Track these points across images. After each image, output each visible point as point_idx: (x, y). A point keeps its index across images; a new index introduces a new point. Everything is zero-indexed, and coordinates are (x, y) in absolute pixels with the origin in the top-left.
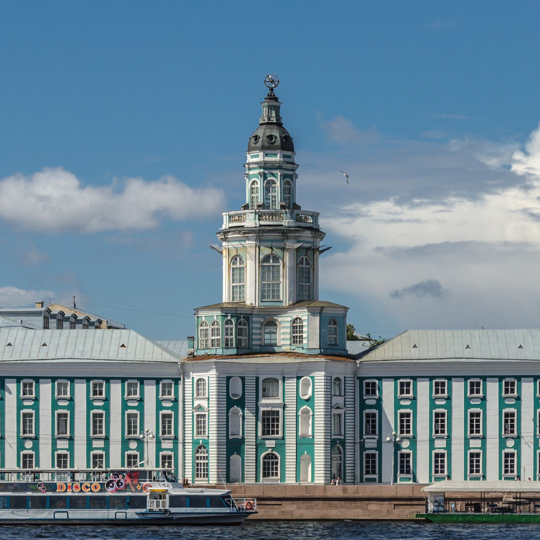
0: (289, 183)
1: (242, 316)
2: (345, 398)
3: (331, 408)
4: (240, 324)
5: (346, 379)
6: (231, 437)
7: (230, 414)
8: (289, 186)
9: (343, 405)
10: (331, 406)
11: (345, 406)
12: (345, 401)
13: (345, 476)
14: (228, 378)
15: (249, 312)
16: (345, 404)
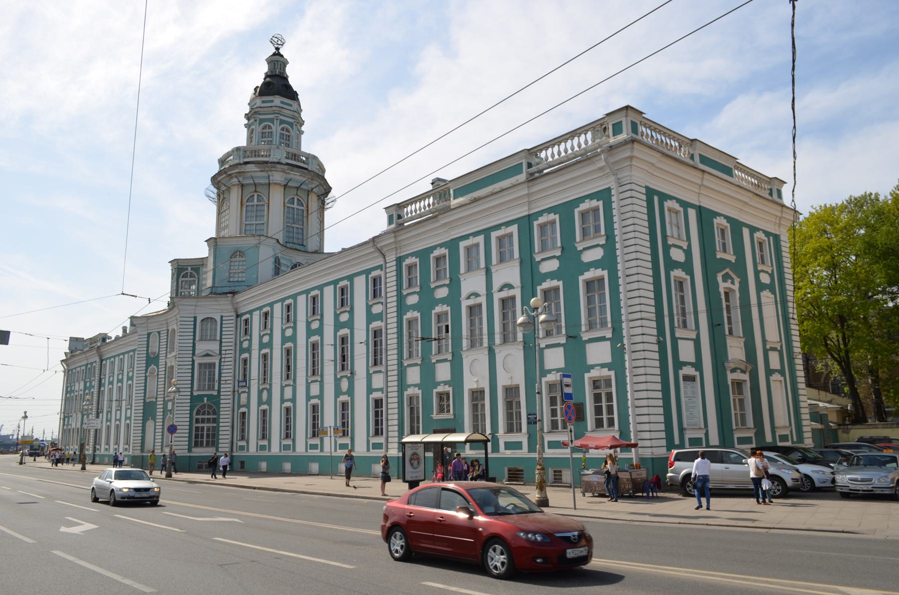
0: (270, 127)
1: (189, 268)
2: (221, 342)
3: (194, 354)
4: (185, 276)
5: (224, 318)
6: (148, 401)
7: (147, 374)
8: (288, 134)
9: (218, 352)
10: (194, 354)
11: (220, 354)
12: (221, 346)
13: (218, 443)
14: (149, 334)
15: (200, 263)
16: (220, 350)
